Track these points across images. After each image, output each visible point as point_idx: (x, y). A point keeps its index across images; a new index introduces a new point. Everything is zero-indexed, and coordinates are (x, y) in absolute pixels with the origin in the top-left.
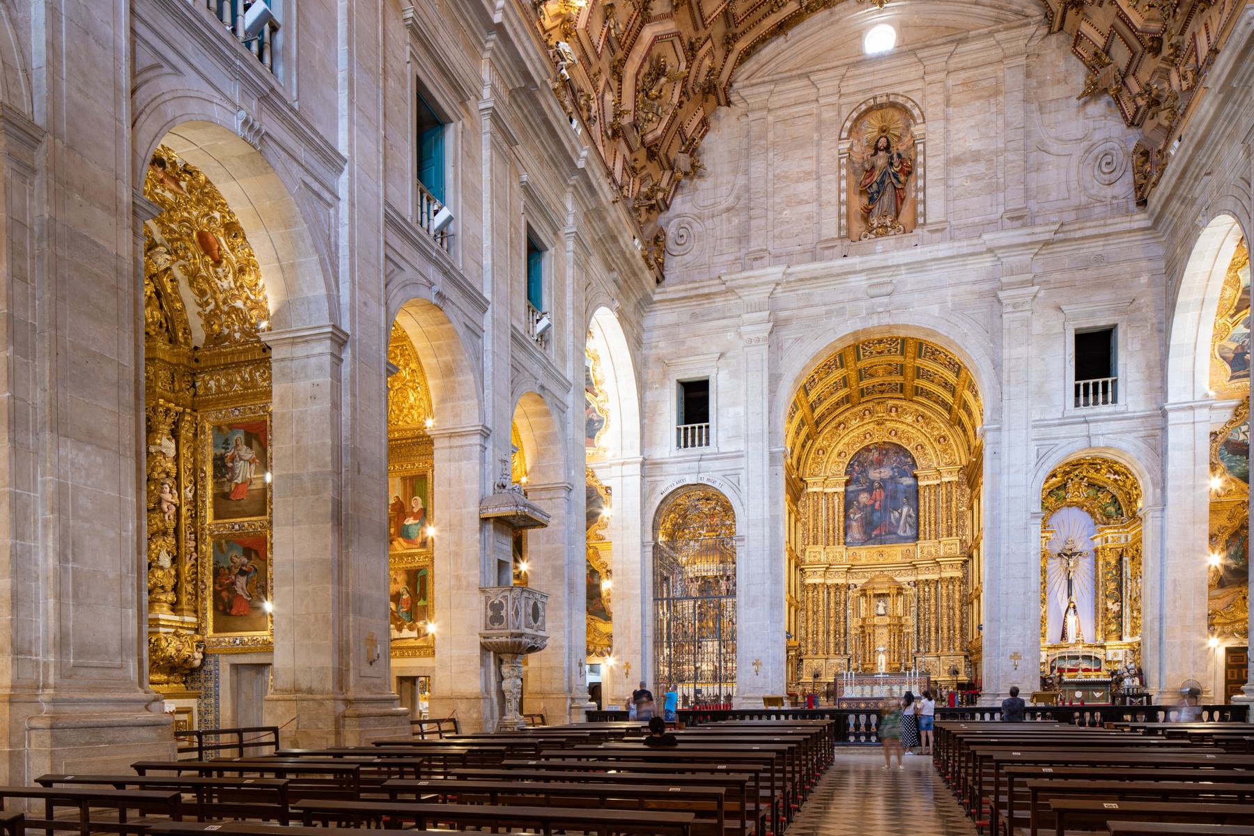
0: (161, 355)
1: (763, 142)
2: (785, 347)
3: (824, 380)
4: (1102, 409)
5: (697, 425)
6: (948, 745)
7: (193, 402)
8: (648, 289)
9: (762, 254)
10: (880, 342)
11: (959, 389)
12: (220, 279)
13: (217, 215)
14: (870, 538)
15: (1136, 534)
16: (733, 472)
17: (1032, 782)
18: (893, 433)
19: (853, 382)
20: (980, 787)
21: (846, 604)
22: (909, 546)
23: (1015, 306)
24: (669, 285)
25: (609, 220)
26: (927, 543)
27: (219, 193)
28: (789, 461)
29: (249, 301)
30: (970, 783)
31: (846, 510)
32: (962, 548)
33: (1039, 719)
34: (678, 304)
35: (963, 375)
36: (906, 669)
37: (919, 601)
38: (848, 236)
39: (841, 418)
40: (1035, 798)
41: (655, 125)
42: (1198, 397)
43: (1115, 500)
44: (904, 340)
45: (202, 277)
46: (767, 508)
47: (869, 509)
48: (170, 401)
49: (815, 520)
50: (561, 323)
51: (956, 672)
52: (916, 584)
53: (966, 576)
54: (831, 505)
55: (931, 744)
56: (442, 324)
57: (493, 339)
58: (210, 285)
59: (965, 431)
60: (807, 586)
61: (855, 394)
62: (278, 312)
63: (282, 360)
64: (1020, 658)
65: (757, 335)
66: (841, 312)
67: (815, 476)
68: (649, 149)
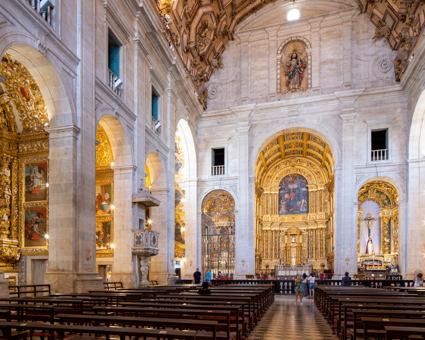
0: (5, 136)
2: (255, 135)
3: (271, 149)
5: (219, 166)
6: (320, 295)
7: (18, 155)
8: (200, 112)
9: (246, 99)
10: (293, 134)
12: (29, 106)
13: (28, 81)
14: (289, 212)
16: (234, 185)
17: (354, 310)
20: (333, 313)
21: (279, 238)
22: (305, 215)
23: (347, 120)
24: (209, 111)
26: (312, 214)
27: (29, 72)
28: (257, 181)
29: (40, 115)
30: (329, 310)
31: (279, 201)
32: (326, 216)
33: (357, 285)
34: (212, 118)
36: (303, 264)
37: (308, 237)
38: (280, 92)
39: (278, 164)
40: (355, 317)
44: (303, 134)
45: (22, 105)
46: (247, 199)
47: (289, 200)
48: (8, 154)
49: (267, 204)
50: (165, 125)
51: (323, 266)
52: (307, 230)
53: (327, 227)
54: (273, 199)
55: (313, 294)
56: (118, 125)
57: (138, 131)
58: (25, 108)
59: (327, 170)
61: (283, 155)
62: (52, 120)
63: (54, 138)
64: (349, 260)
65: (244, 131)
66: (278, 122)
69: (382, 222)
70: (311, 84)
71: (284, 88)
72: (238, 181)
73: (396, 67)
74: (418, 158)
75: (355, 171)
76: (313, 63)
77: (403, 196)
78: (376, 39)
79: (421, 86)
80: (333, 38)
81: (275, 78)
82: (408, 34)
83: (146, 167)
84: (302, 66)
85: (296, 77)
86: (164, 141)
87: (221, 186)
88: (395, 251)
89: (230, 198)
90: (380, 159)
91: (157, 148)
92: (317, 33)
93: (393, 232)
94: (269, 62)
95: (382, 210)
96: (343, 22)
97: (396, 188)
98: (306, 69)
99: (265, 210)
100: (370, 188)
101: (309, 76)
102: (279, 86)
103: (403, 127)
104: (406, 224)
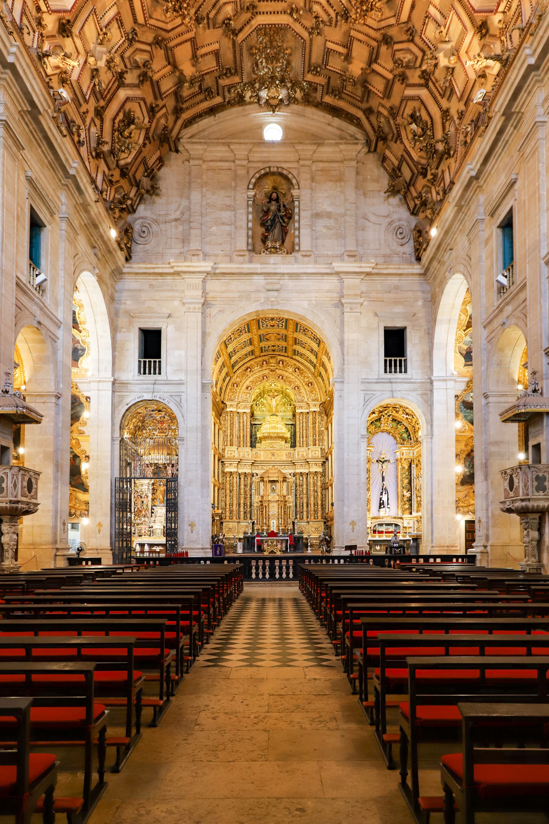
1: (199, 181)
2: (212, 315)
3: (238, 339)
4: (398, 375)
5: (152, 360)
8: (120, 264)
9: (198, 252)
10: (272, 319)
16: (177, 394)
25: (92, 213)
26: (302, 449)
28: (215, 389)
35: (322, 346)
37: (296, 486)
38: (253, 250)
39: (248, 365)
41: (126, 155)
42: (448, 374)
43: (407, 430)
44: (287, 320)
46: (199, 419)
53: (324, 472)
54: (241, 421)
60: (226, 473)
68: (122, 170)
69: (400, 467)
70: (299, 245)
71: (259, 245)
72: (183, 388)
73: (416, 241)
74: (444, 375)
75: (362, 387)
76: (302, 214)
78: (389, 194)
79: (447, 273)
80: (331, 181)
81: (245, 226)
83: (17, 351)
84: (285, 215)
85: (277, 231)
86: (51, 308)
87: (154, 394)
89: (169, 416)
90: (395, 372)
91: (37, 319)
93: (415, 483)
94: (235, 200)
95: (400, 448)
96: (345, 160)
97: (418, 417)
98: (291, 221)
99: (229, 439)
100: (383, 413)
101: (297, 233)
102: (250, 240)
103: (426, 327)
104: (432, 471)
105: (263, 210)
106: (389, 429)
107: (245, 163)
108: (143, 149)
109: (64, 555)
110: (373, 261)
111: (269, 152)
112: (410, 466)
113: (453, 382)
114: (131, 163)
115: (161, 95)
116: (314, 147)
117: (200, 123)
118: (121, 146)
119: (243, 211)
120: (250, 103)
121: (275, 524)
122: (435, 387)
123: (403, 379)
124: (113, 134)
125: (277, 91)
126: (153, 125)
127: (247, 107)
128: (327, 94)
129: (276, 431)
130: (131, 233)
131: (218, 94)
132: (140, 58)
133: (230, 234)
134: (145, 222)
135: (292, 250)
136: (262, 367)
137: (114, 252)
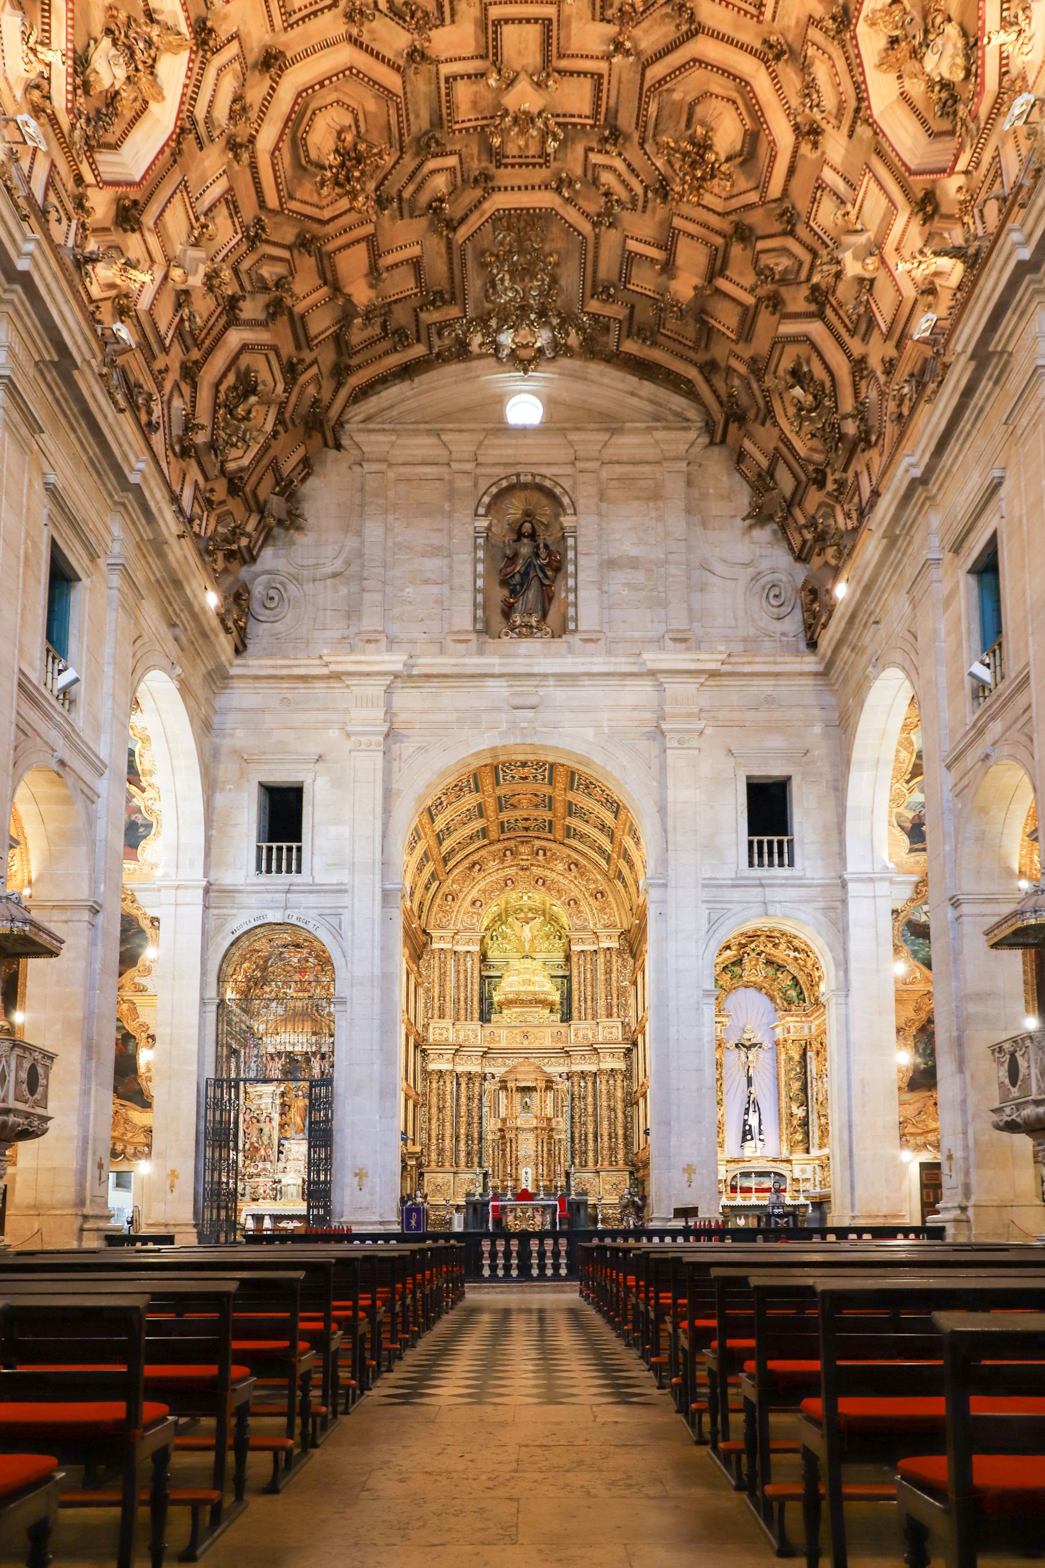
1: (381, 501)
2: (405, 756)
4: (777, 871)
5: (284, 845)
8: (223, 659)
9: (377, 636)
10: (524, 764)
11: (618, 833)
15: (819, 1025)
16: (333, 911)
18: (540, 881)
19: (491, 811)
21: (480, 1100)
26: (584, 1024)
28: (408, 904)
34: (264, 684)
37: (573, 1099)
41: (240, 453)
42: (878, 868)
44: (552, 766)
46: (377, 961)
52: (569, 1076)
53: (629, 1069)
54: (462, 968)
60: (430, 1073)
67: (443, 928)
68: (231, 481)
69: (783, 1057)
70: (576, 620)
71: (497, 620)
72: (345, 900)
73: (807, 609)
76: (582, 561)
77: (837, 977)
80: (638, 498)
81: (469, 586)
82: (832, 522)
84: (549, 564)
85: (532, 594)
87: (288, 912)
88: (821, 1147)
89: (317, 957)
90: (771, 864)
92: (592, 475)
94: (450, 537)
95: (783, 1018)
96: (665, 459)
98: (560, 575)
99: (436, 1006)
100: (748, 950)
101: (571, 597)
102: (480, 613)
105: (505, 556)
106: (759, 979)
107: (469, 466)
108: (273, 442)
109: (98, 1230)
110: (723, 648)
111: (516, 446)
112: (804, 1056)
113: (887, 884)
114: (248, 467)
115: (308, 339)
116: (605, 436)
117: (383, 394)
118: (230, 436)
119: (468, 558)
120: (480, 356)
121: (529, 1175)
122: (850, 894)
123: (786, 878)
124: (215, 412)
125: (533, 333)
126: (293, 398)
127: (474, 364)
128: (628, 336)
129: (531, 988)
130: (248, 600)
131: (418, 340)
132: (268, 272)
133: (439, 601)
134: (274, 580)
135: (562, 630)
136: (502, 861)
137: (212, 635)
